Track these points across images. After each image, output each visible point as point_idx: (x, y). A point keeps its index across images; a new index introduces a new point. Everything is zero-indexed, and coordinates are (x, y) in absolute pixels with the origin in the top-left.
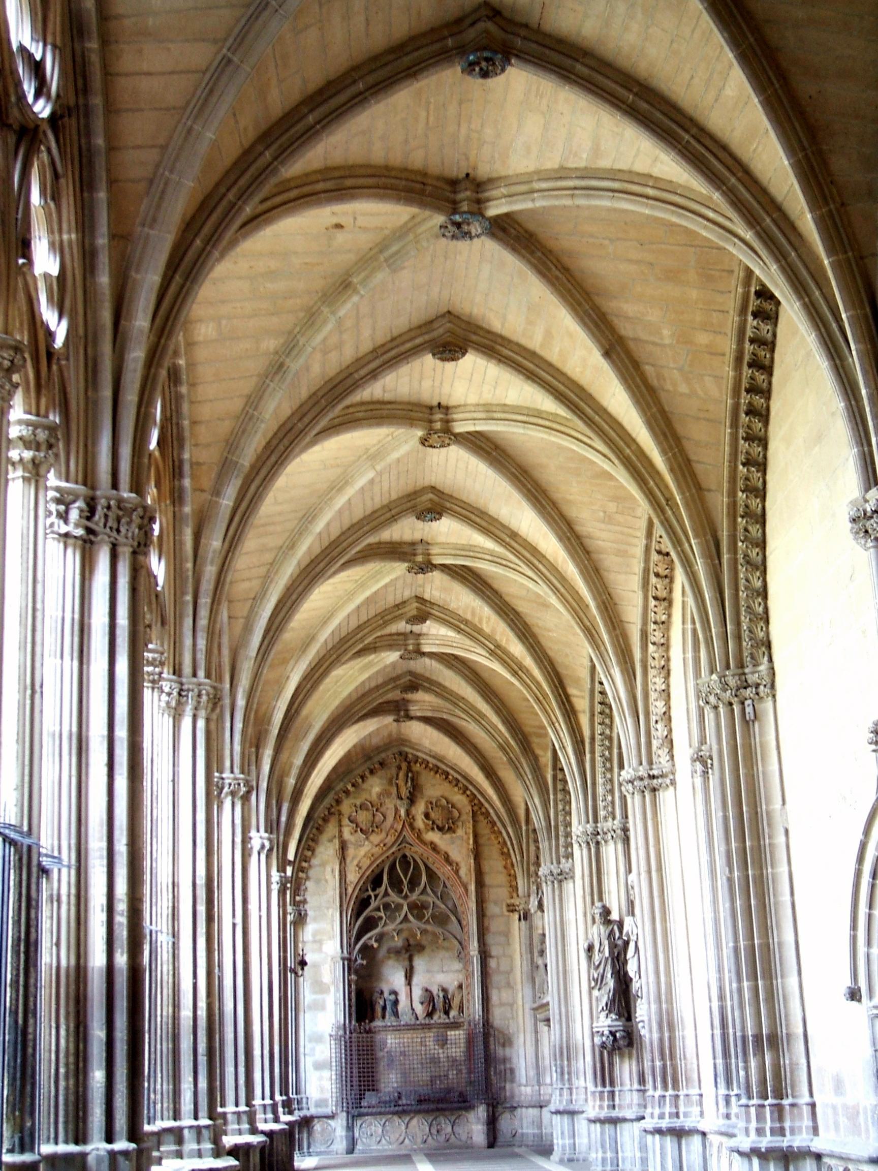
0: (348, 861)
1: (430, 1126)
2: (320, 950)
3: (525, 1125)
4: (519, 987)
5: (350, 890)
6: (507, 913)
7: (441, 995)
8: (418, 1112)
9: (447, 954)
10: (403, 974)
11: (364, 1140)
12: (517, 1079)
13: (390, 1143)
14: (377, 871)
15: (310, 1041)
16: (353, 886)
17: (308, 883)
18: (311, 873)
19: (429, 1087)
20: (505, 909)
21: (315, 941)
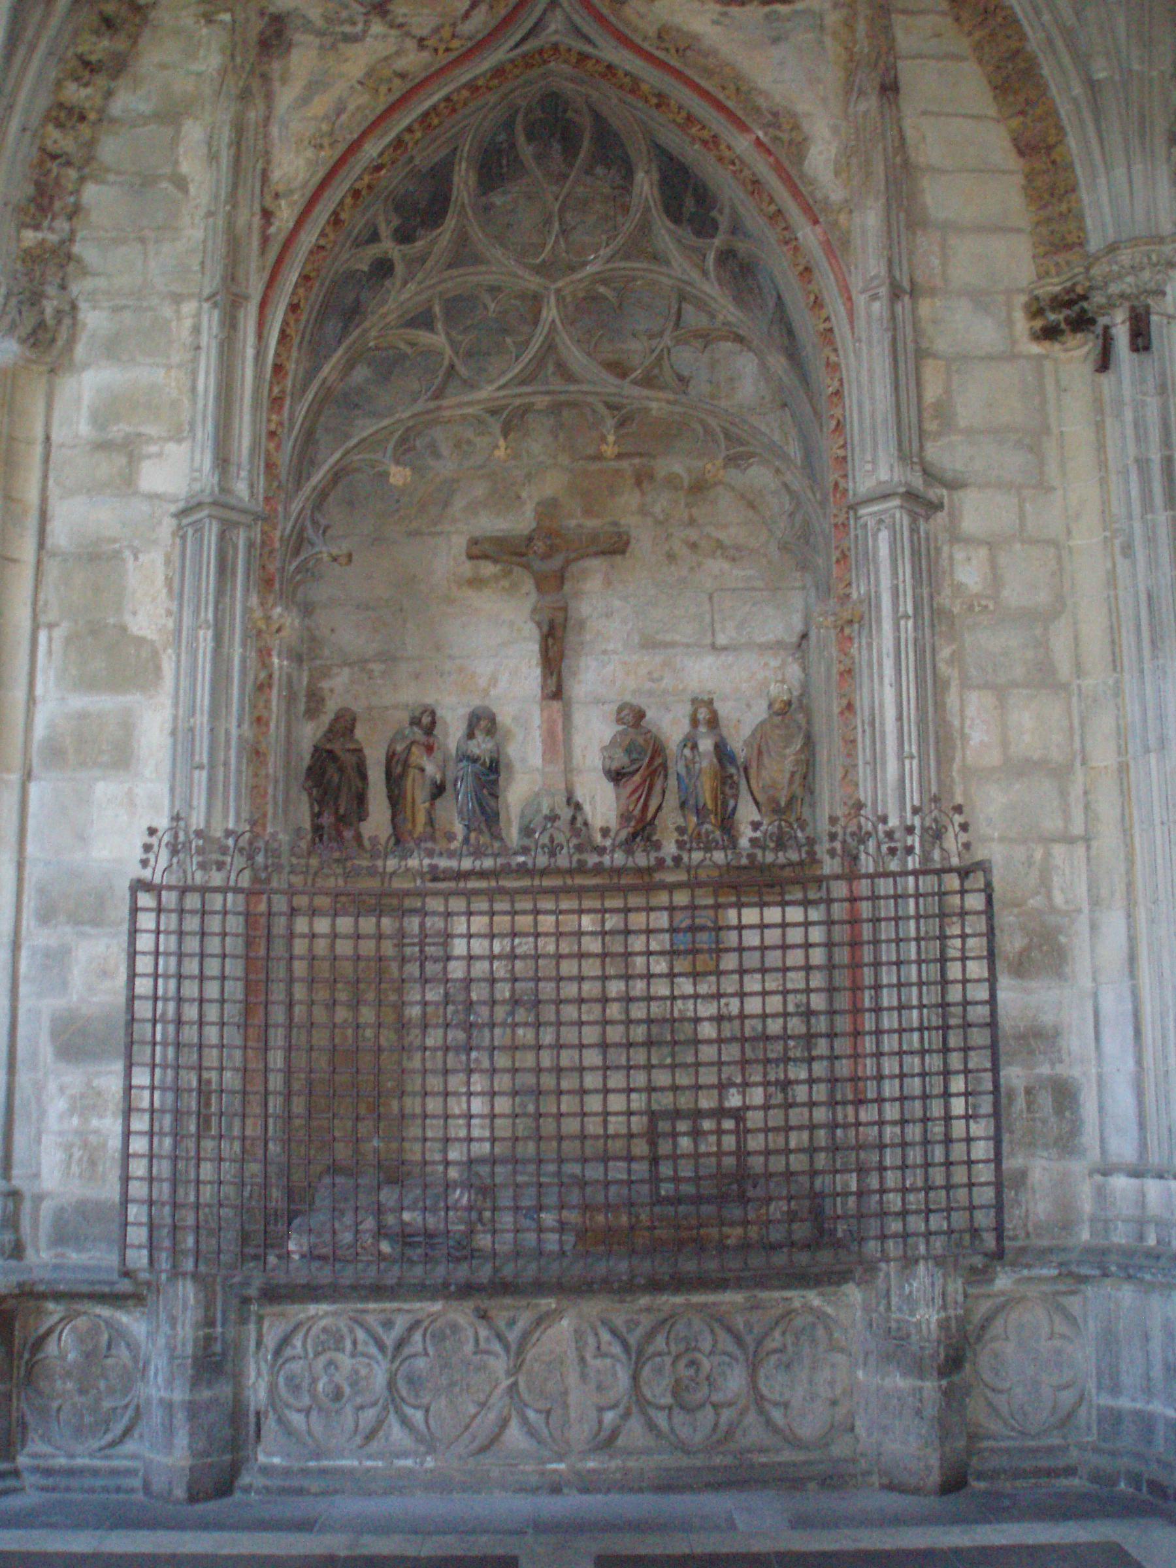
0: (286, 97)
1: (638, 1358)
2: (127, 482)
3: (1130, 1378)
4: (1096, 679)
5: (286, 216)
6: (1036, 349)
7: (706, 744)
8: (584, 1288)
9: (738, 574)
10: (533, 648)
11: (297, 1419)
12: (1089, 1136)
13: (428, 1443)
14: (425, 157)
15: (46, 917)
16: (300, 198)
17: (90, 192)
18: (110, 149)
19: (641, 1169)
20: (1022, 325)
21: (103, 446)
